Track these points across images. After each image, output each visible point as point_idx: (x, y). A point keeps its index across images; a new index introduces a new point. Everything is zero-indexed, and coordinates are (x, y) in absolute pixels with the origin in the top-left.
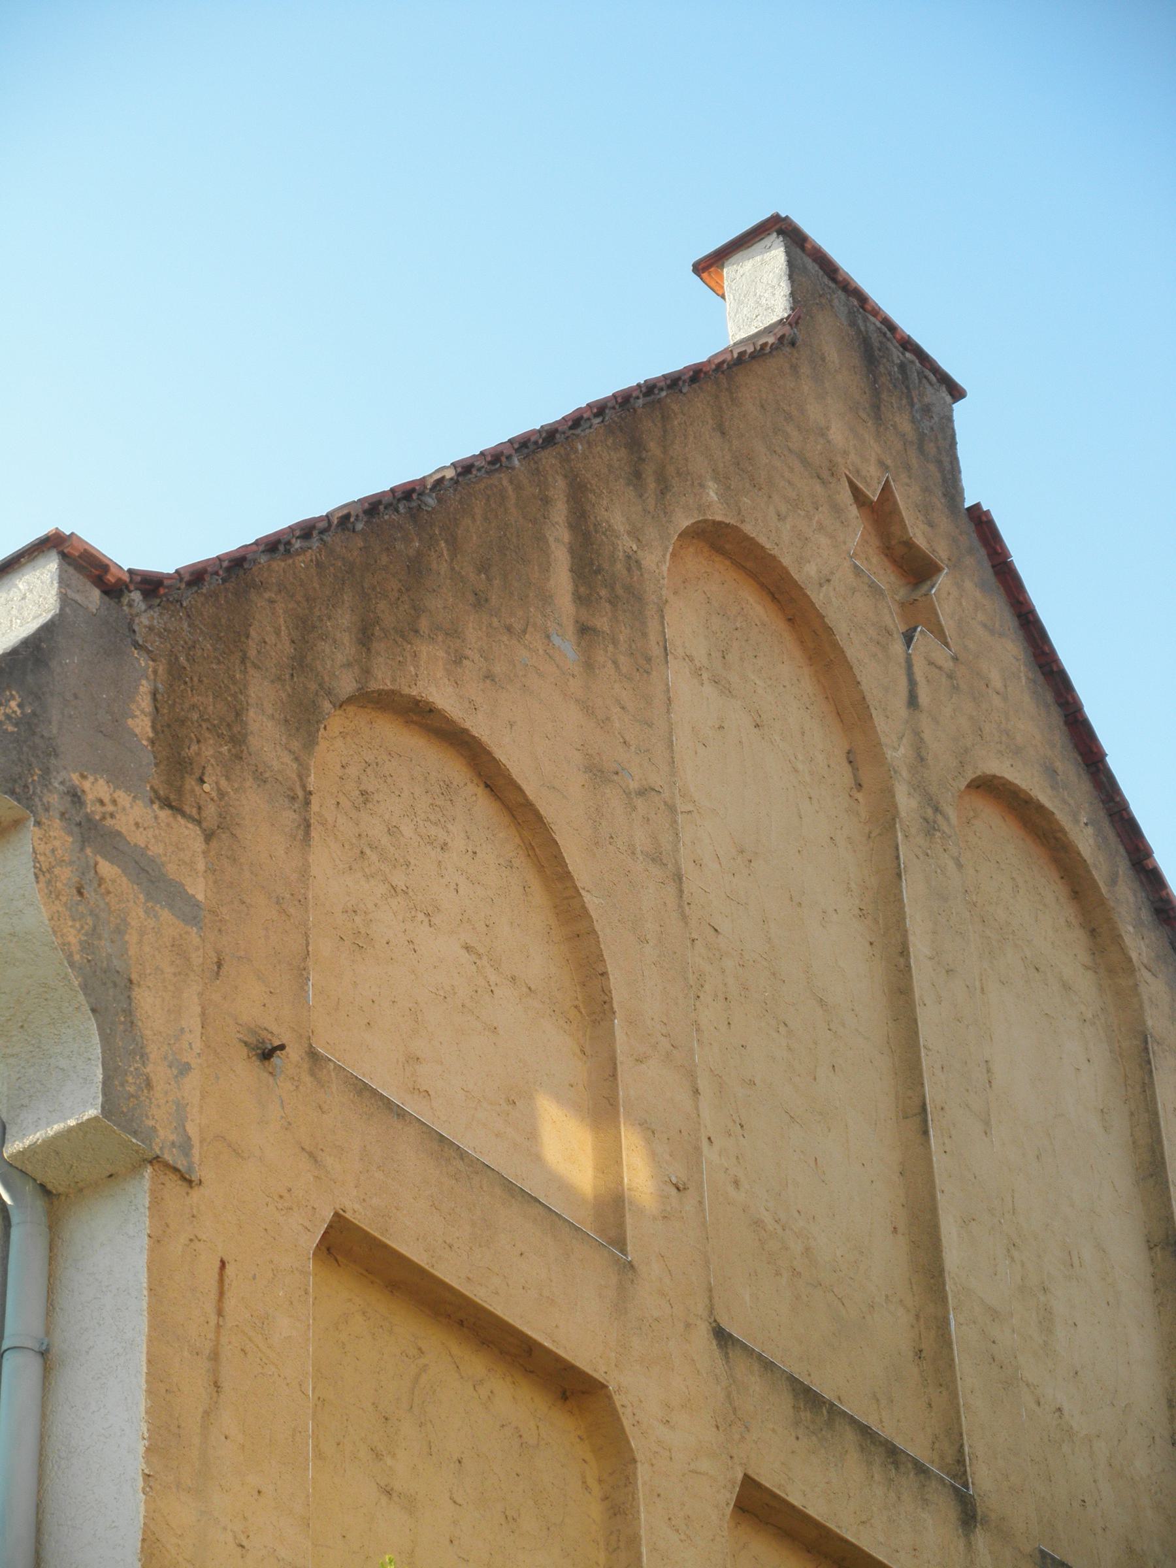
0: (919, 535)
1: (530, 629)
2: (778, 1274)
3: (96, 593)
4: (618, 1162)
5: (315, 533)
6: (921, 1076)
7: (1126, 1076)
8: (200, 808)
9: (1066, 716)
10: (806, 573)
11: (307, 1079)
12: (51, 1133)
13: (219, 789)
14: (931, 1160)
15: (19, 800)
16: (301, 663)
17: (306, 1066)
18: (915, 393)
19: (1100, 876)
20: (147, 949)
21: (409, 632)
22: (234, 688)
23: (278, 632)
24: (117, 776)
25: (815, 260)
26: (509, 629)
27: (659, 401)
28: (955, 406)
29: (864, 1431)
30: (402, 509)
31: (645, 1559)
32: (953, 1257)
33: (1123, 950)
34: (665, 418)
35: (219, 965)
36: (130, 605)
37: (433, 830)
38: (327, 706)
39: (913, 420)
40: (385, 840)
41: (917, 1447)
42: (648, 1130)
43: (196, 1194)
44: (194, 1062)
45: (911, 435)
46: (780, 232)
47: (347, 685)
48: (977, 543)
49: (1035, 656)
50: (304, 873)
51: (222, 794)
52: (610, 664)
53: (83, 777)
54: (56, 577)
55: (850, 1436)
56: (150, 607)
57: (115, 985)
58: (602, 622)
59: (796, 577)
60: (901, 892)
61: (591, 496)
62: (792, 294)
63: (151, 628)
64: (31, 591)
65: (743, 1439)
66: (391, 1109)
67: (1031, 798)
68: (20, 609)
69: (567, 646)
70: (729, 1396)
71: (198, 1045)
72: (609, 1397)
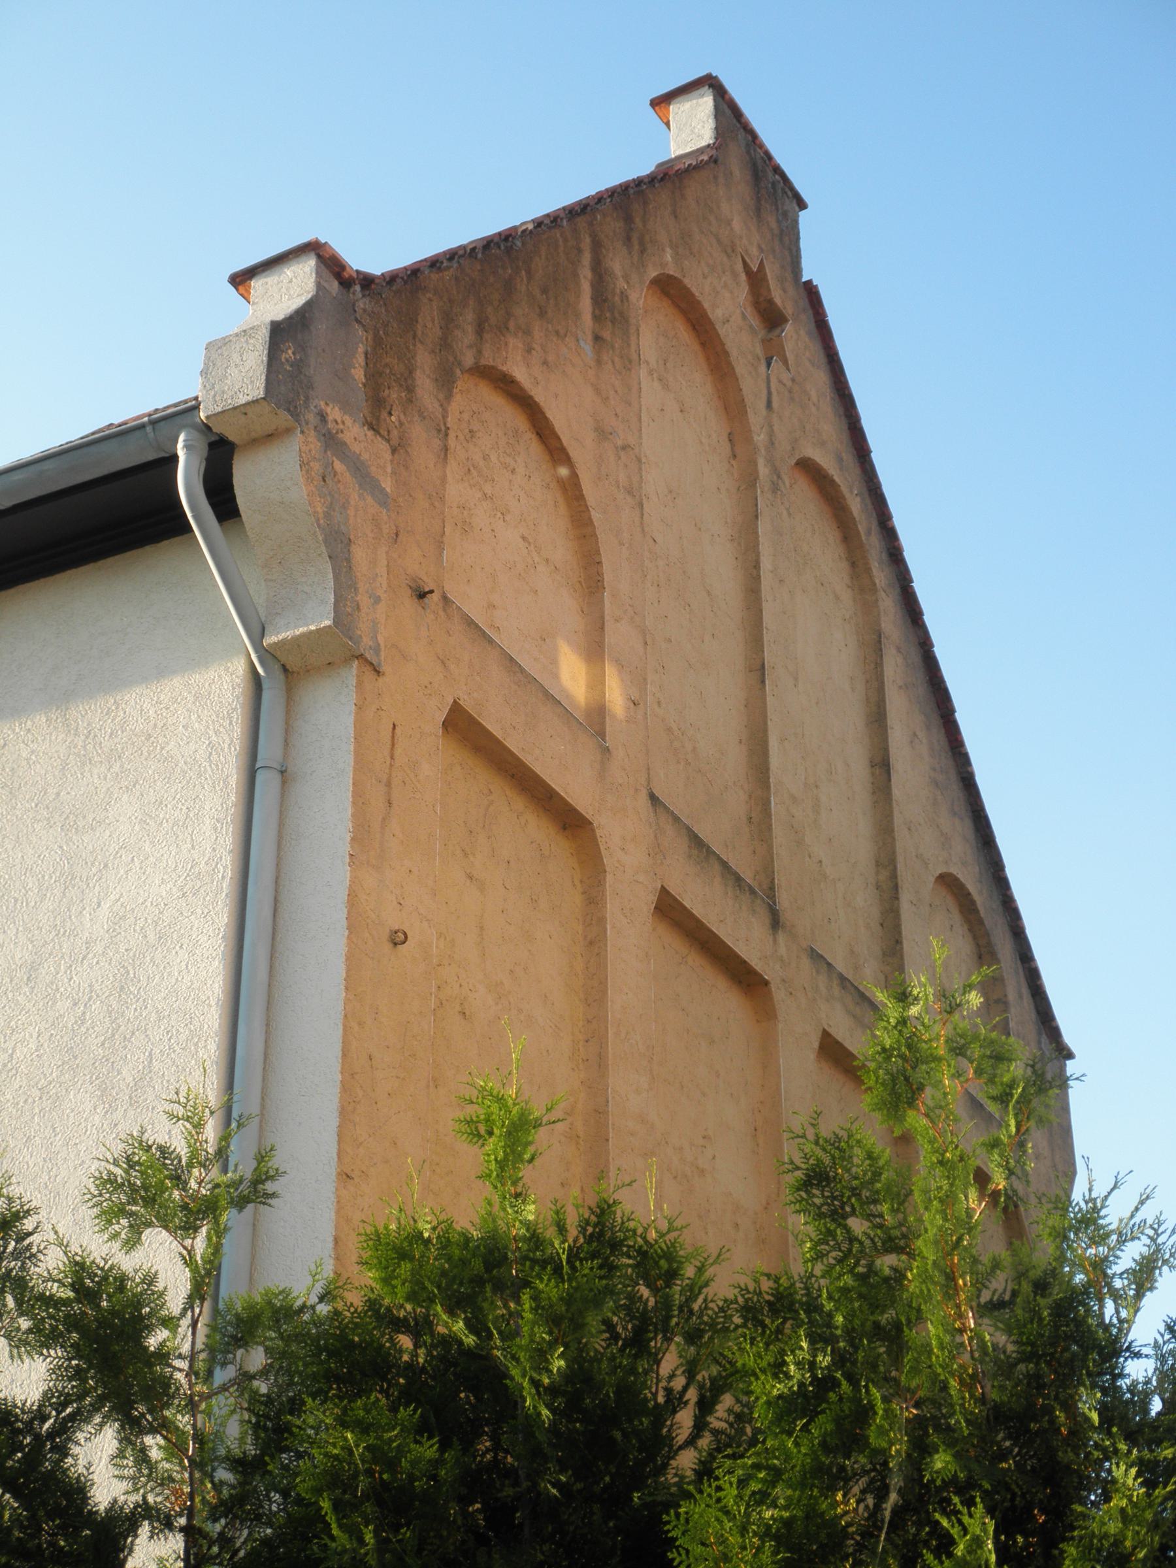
0: (777, 297)
1: (569, 334)
2: (678, 762)
3: (336, 284)
4: (603, 683)
5: (456, 257)
6: (763, 646)
7: (865, 658)
8: (389, 432)
9: (850, 424)
10: (717, 314)
11: (441, 613)
12: (297, 633)
13: (400, 421)
14: (765, 699)
15: (292, 415)
16: (445, 344)
17: (441, 605)
18: (779, 202)
19: (862, 528)
20: (359, 521)
21: (502, 329)
22: (409, 355)
23: (433, 321)
24: (345, 407)
25: (729, 107)
26: (557, 333)
27: (642, 191)
28: (801, 213)
29: (724, 864)
30: (502, 247)
31: (609, 933)
32: (774, 761)
33: (871, 577)
34: (645, 203)
35: (397, 535)
36: (354, 294)
37: (508, 460)
38: (458, 372)
39: (778, 221)
40: (482, 463)
41: (748, 876)
42: (620, 666)
43: (381, 680)
44: (383, 596)
45: (776, 231)
46: (711, 86)
47: (469, 360)
48: (808, 306)
49: (835, 383)
50: (444, 479)
51: (401, 424)
52: (610, 362)
53: (327, 404)
54: (314, 270)
55: (717, 867)
56: (364, 296)
57: (342, 542)
58: (606, 335)
59: (711, 316)
60: (757, 527)
61: (603, 250)
62: (716, 128)
63: (365, 310)
64: (296, 278)
65: (662, 863)
66: (484, 637)
67: (828, 474)
68: (288, 289)
69: (587, 347)
70: (656, 836)
71: (385, 585)
72: (593, 830)
